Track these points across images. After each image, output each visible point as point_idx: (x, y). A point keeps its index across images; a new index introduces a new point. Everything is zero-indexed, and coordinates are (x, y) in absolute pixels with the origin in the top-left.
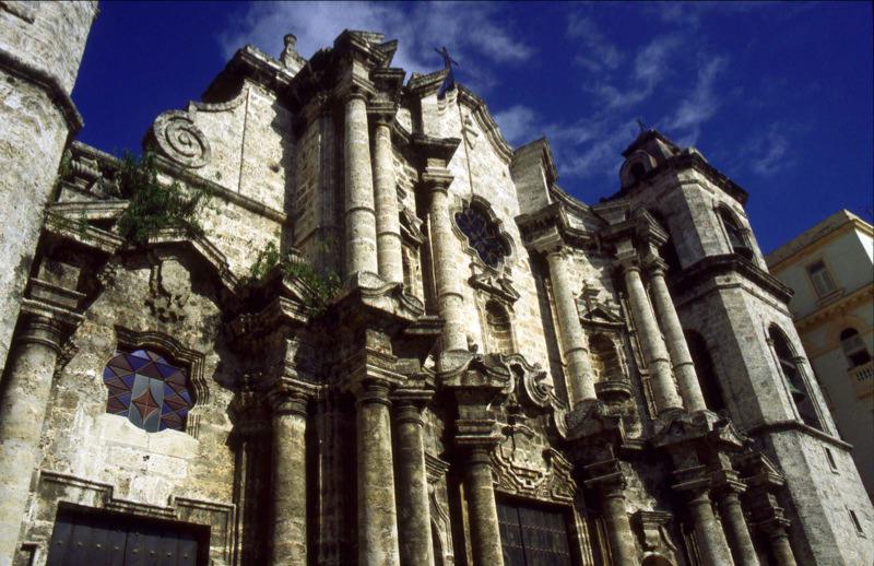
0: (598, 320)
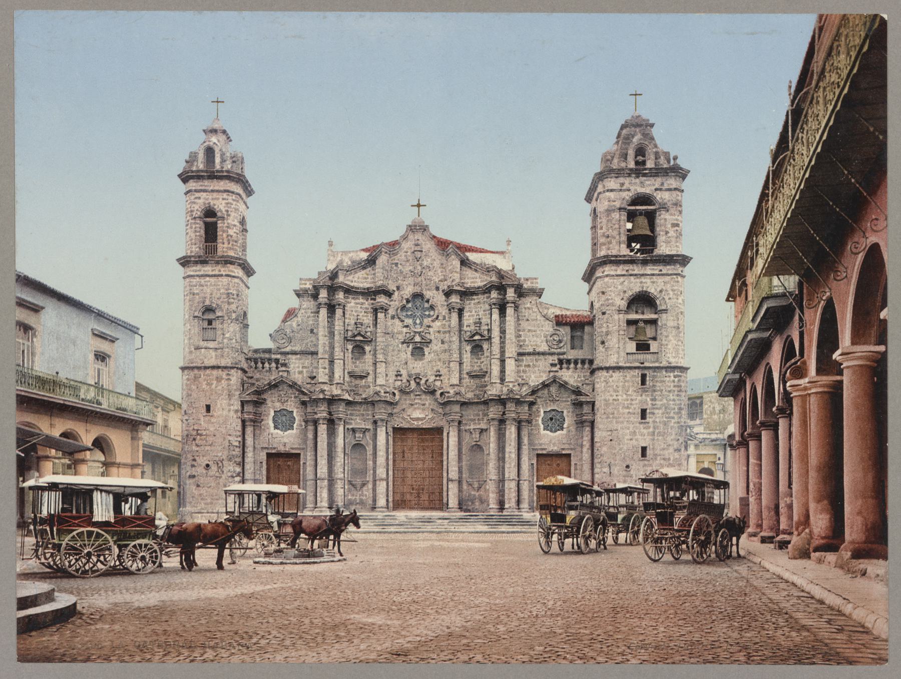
0: (477, 337)
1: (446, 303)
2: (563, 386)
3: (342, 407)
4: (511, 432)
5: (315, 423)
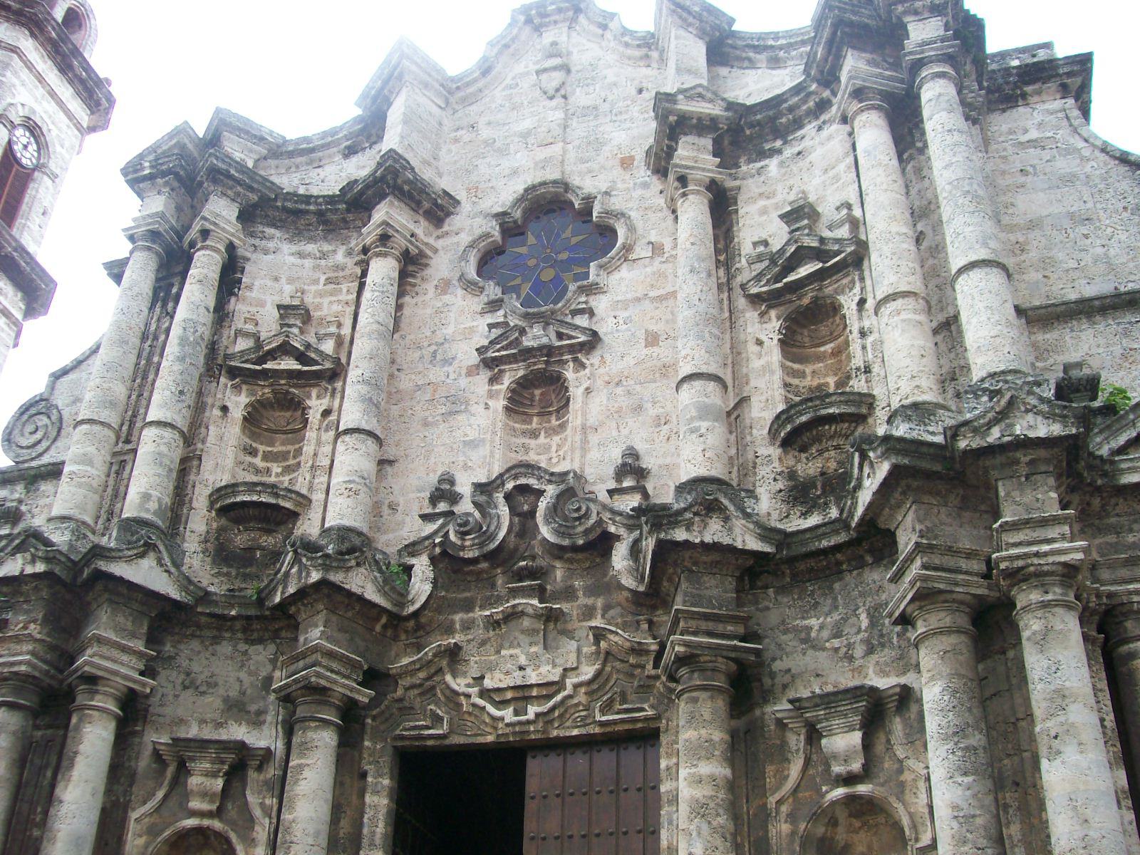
0: (803, 271)
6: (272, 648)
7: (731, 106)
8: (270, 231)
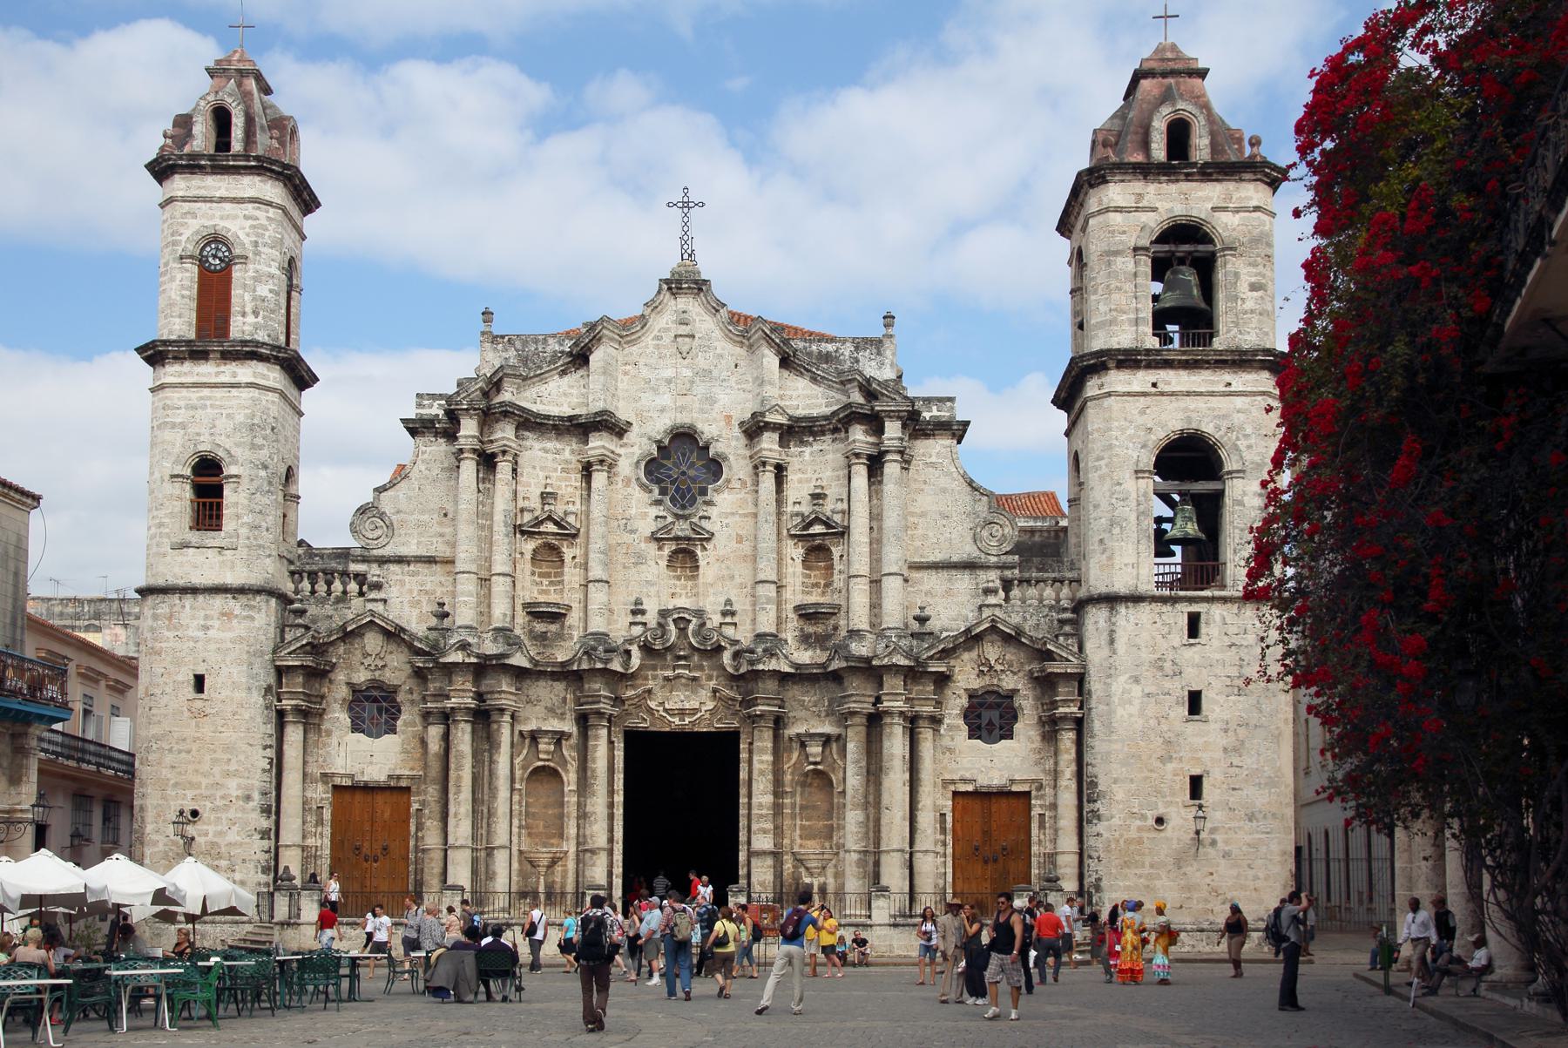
0: (818, 529)
1: (748, 453)
2: (1012, 639)
3: (506, 685)
4: (895, 744)
5: (446, 717)
6: (564, 683)
7: (791, 418)
8: (527, 433)
